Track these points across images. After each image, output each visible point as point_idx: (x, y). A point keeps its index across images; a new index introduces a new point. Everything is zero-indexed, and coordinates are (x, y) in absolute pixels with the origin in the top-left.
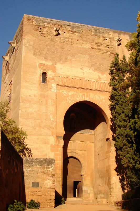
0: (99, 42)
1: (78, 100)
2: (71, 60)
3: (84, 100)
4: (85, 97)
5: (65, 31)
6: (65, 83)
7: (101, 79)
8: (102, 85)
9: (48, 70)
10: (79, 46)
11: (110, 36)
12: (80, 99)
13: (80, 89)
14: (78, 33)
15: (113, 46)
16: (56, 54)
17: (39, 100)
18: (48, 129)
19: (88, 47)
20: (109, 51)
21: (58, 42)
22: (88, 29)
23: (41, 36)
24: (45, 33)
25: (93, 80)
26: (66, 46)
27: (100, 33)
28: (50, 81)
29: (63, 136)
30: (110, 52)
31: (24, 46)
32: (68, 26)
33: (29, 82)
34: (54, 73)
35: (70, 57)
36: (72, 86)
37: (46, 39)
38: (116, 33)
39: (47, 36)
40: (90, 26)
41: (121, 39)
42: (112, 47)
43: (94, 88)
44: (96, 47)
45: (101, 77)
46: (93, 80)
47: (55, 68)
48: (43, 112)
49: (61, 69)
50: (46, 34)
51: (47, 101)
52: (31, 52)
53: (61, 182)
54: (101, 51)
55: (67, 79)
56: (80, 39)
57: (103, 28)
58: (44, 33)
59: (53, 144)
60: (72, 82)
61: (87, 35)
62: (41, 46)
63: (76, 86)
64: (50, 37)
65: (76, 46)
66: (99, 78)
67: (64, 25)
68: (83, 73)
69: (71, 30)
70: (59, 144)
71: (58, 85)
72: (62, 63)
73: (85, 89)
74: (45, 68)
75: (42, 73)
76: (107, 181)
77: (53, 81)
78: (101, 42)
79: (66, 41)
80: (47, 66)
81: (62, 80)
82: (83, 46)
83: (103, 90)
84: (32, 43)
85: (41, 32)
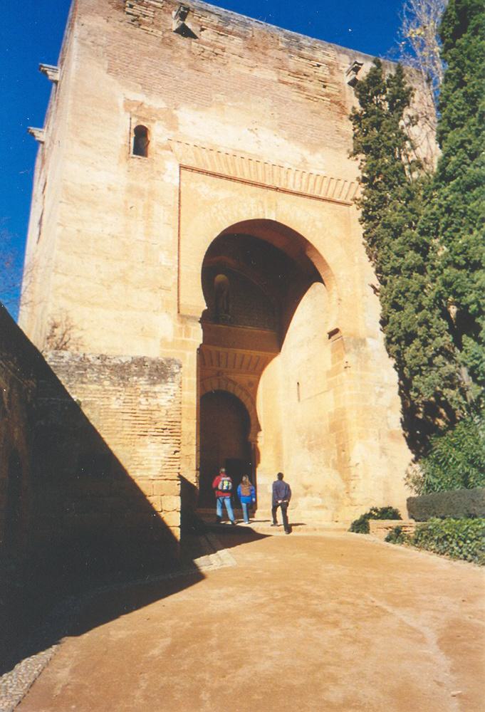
0: (300, 69)
1: (245, 216)
2: (221, 104)
3: (261, 217)
4: (263, 207)
5: (203, 27)
6: (206, 165)
7: (308, 165)
8: (312, 181)
9: (153, 121)
10: (246, 71)
11: (327, 58)
12: (251, 214)
13: (248, 187)
14: (240, 36)
15: (338, 84)
16: (177, 81)
17: (126, 202)
18: (151, 291)
19: (270, 78)
20: (328, 95)
21: (184, 52)
22: (268, 31)
23: (132, 26)
24: (146, 19)
25: (287, 165)
26: (205, 65)
27: (301, 48)
28: (159, 151)
29: (200, 316)
30: (329, 100)
31: (78, 41)
32: (213, 17)
33: (90, 146)
34: (172, 133)
35: (218, 95)
36: (227, 174)
37: (148, 37)
38: (345, 53)
39: (151, 29)
40: (274, 27)
41: (362, 65)
42: (336, 86)
43: (290, 188)
44: (292, 82)
45: (310, 158)
46: (287, 165)
47: (174, 117)
48: (138, 240)
49: (193, 123)
50: (149, 24)
51: (149, 207)
52: (99, 63)
53: (197, 459)
54: (305, 93)
55: (214, 153)
56: (247, 53)
57: (310, 38)
58: (144, 19)
59: (170, 339)
60: (226, 162)
61: (265, 48)
62: (131, 52)
63: (239, 176)
64: (161, 33)
65: (236, 68)
66: (304, 160)
67: (201, 9)
68: (258, 142)
69: (220, 25)
70: (187, 339)
71: (181, 167)
72: (197, 109)
73: (263, 186)
74: (143, 114)
75: (134, 127)
76: (334, 457)
77: (169, 152)
78: (305, 70)
79: (206, 53)
80: (150, 108)
81: (195, 154)
82: (256, 73)
83: (316, 194)
84: (104, 40)
85: (132, 14)
